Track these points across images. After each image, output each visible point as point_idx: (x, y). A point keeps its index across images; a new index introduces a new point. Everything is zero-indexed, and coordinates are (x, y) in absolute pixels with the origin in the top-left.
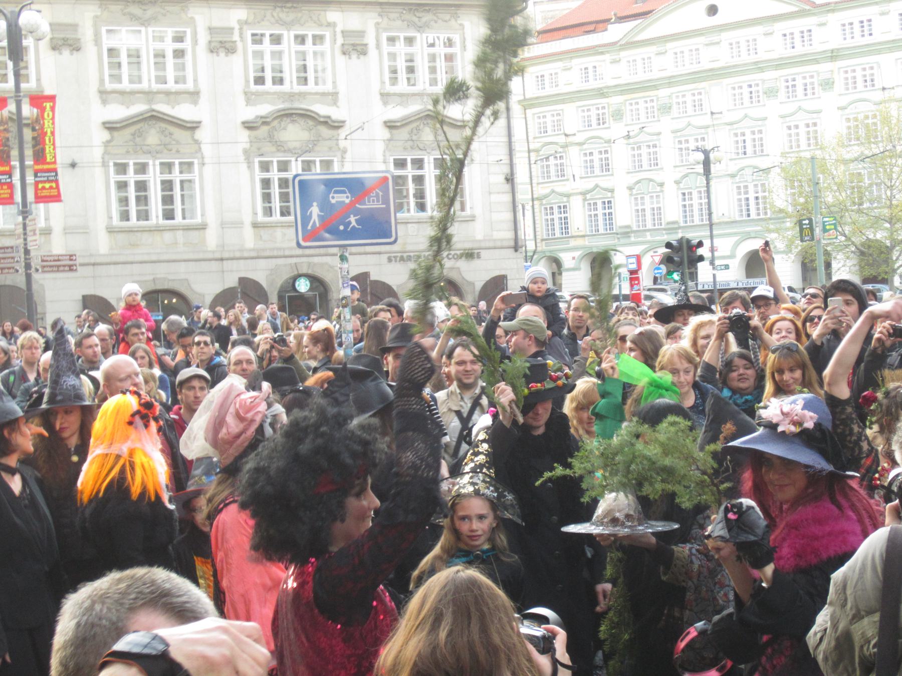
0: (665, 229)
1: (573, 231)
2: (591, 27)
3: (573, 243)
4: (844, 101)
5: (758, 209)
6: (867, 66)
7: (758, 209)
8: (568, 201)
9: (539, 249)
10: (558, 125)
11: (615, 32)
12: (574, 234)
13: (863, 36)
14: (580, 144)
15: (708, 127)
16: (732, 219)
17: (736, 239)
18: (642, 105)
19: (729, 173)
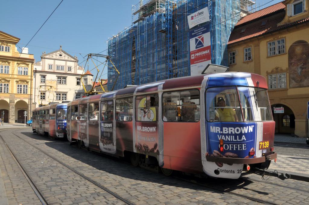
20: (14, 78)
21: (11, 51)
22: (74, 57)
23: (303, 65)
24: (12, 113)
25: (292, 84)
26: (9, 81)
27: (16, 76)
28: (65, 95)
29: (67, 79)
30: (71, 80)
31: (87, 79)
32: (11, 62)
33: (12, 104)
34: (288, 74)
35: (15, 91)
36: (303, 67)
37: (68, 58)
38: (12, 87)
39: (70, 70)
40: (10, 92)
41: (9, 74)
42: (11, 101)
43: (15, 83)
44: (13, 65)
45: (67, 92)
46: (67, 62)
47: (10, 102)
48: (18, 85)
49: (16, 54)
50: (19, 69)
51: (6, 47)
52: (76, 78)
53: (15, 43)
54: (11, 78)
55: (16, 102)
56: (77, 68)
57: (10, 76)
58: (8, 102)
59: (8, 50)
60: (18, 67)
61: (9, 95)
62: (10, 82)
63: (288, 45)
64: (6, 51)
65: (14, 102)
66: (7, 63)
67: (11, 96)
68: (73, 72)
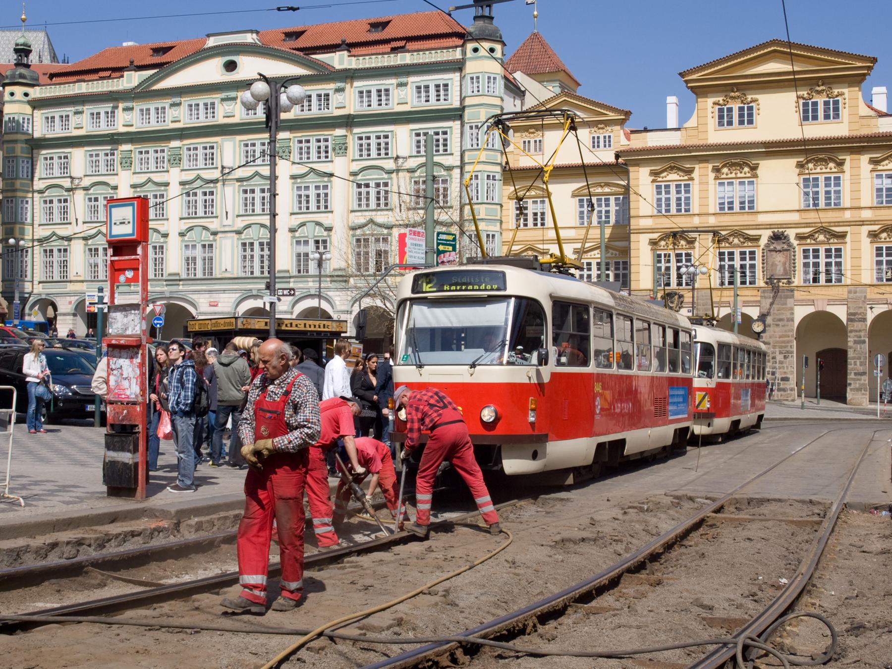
0: (166, 280)
1: (71, 276)
2: (107, 74)
3: (71, 287)
4: (356, 167)
5: (262, 267)
6: (382, 134)
7: (262, 267)
8: (69, 245)
9: (35, 291)
10: (65, 167)
11: (131, 80)
12: (73, 279)
13: (380, 105)
14: (86, 189)
15: (215, 181)
16: (235, 276)
17: (238, 295)
18: (152, 155)
19: (235, 229)
20: (862, 223)
21: (844, 113)
24: (855, 364)
26: (843, 236)
27: (866, 215)
32: (848, 158)
33: (857, 325)
35: (868, 275)
38: (856, 258)
40: (847, 280)
41: (842, 206)
42: (854, 314)
43: (866, 241)
44: (856, 167)
47: (851, 317)
48: (879, 249)
49: (865, 121)
50: (879, 181)
51: (826, 103)
53: (856, 80)
54: (849, 223)
55: (870, 317)
57: (848, 215)
58: (844, 318)
59: (833, 112)
60: (875, 174)
61: (846, 289)
62: (848, 239)
64: (827, 117)
65: (864, 320)
66: (832, 165)
67: (851, 295)
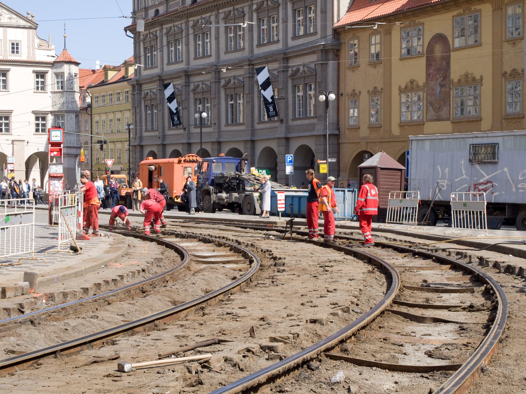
22: (26, 15)
23: (442, 81)
25: (430, 114)
28: (7, 118)
29: (10, 75)
30: (21, 78)
31: (64, 73)
34: (425, 94)
36: (442, 83)
37: (10, 18)
39: (17, 52)
45: (11, 112)
46: (8, 29)
52: (34, 72)
56: (36, 46)
63: (428, 37)
68: (23, 56)
